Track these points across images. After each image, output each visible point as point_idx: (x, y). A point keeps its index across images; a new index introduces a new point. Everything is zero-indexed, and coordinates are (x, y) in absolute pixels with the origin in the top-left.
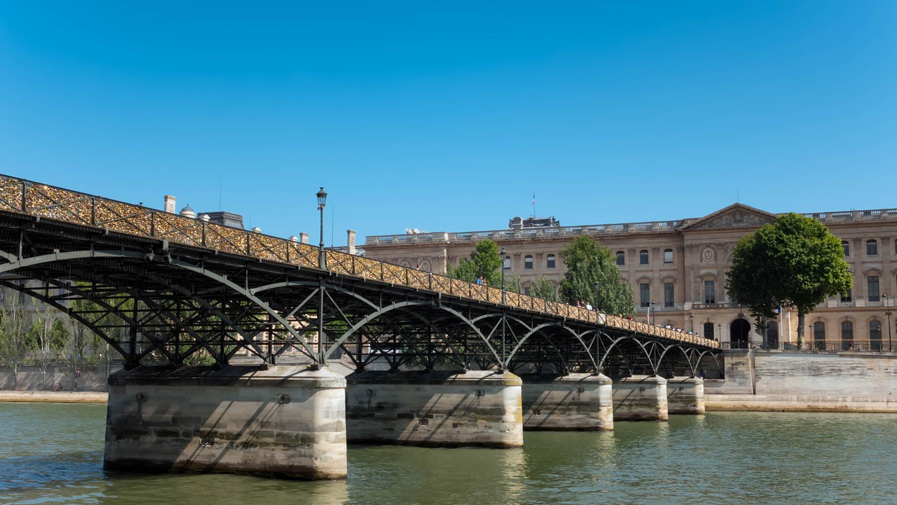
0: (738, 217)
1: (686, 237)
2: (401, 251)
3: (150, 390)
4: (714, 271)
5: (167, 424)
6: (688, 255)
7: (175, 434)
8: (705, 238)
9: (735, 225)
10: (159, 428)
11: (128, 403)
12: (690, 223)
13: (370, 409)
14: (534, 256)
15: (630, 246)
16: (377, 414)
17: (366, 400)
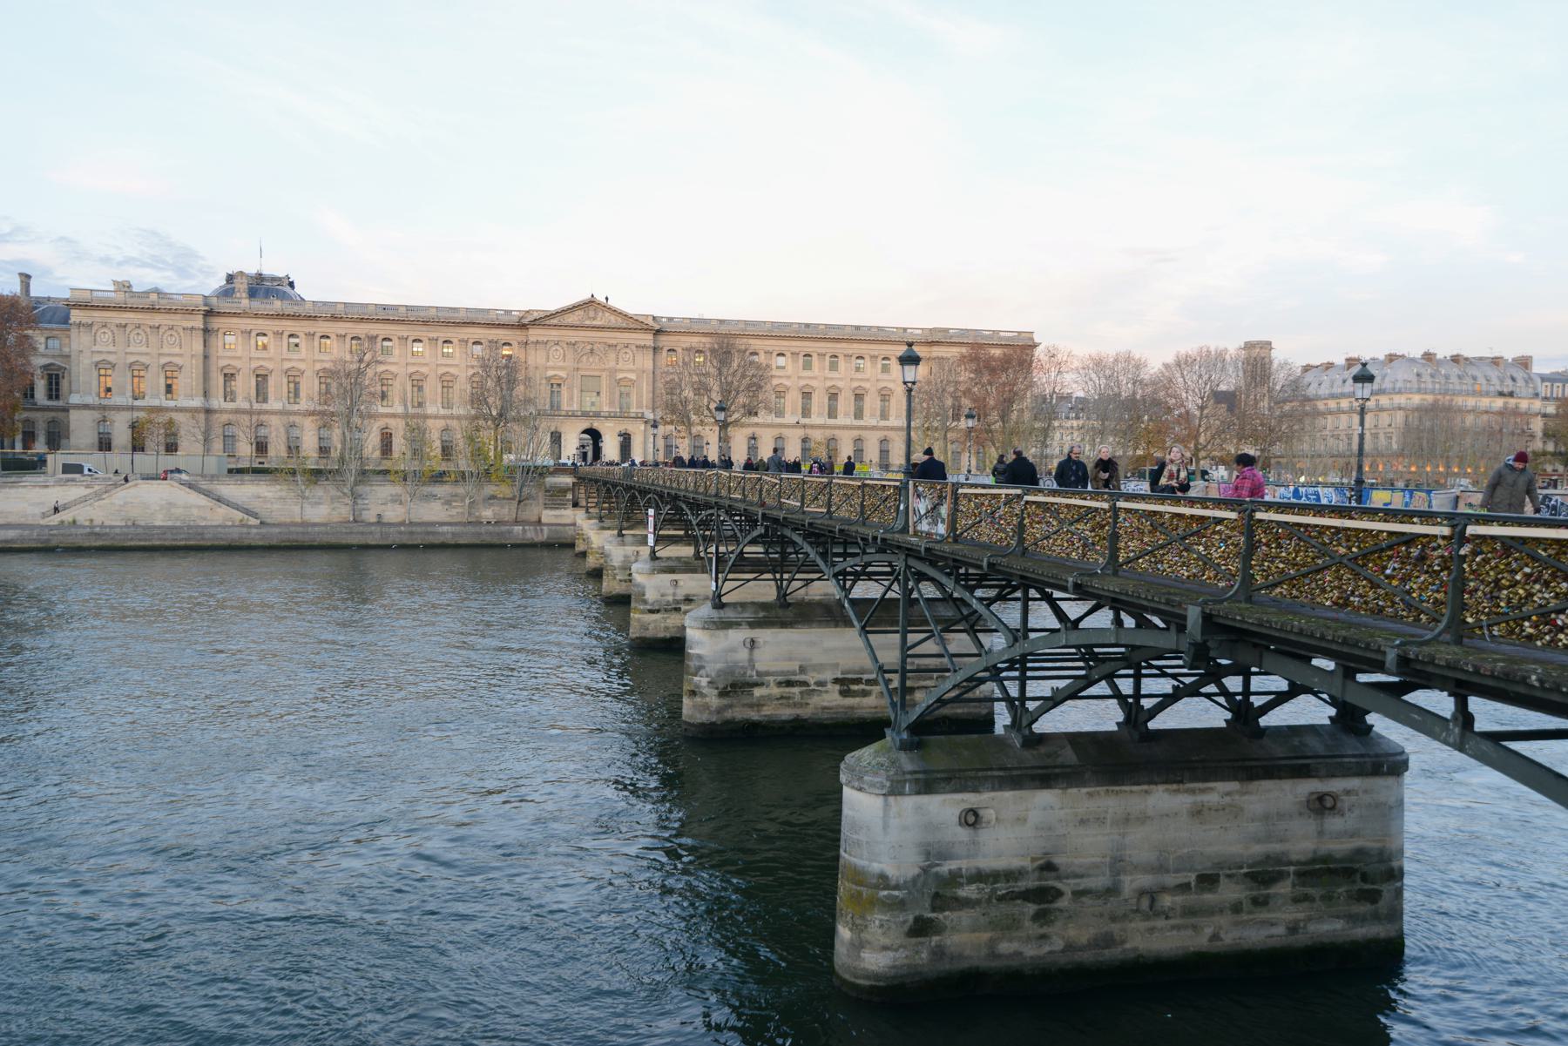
0: (592, 314)
1: (531, 331)
2: (131, 315)
3: (764, 635)
4: (563, 374)
5: (794, 673)
6: (531, 351)
7: (805, 684)
8: (554, 334)
9: (588, 323)
10: (780, 678)
11: (733, 650)
12: (536, 315)
13: (678, 602)
14: (333, 336)
15: (462, 336)
16: (684, 608)
17: (671, 591)
